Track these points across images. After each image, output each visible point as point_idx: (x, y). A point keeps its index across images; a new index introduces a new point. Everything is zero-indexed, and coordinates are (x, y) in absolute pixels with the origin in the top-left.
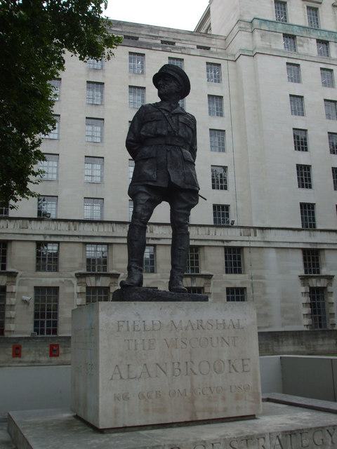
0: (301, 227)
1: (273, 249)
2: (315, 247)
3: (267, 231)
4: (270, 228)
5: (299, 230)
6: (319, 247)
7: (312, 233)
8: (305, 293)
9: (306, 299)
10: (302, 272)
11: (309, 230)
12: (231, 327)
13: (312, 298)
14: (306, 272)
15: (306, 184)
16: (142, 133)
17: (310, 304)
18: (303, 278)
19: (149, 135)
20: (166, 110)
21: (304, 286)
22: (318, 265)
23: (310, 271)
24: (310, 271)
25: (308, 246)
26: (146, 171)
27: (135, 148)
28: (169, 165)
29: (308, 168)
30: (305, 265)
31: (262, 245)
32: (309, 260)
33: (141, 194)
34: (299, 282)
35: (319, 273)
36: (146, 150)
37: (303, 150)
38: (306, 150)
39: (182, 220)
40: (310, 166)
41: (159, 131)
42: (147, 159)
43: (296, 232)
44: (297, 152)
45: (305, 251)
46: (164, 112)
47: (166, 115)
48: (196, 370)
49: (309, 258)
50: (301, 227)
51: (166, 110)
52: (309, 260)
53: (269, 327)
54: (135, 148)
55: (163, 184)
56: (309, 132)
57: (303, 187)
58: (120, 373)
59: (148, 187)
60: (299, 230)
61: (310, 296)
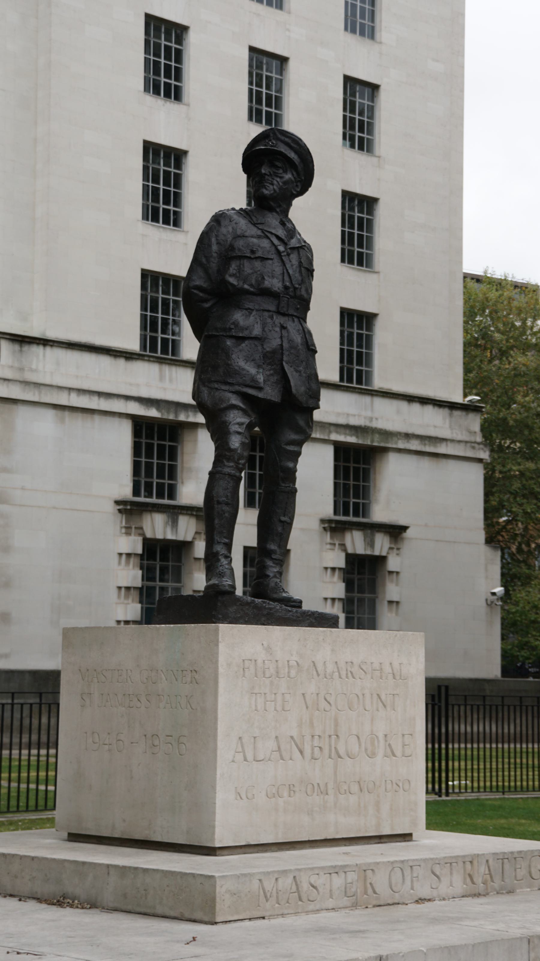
0: (134, 346)
1: (50, 413)
2: (171, 417)
3: (38, 350)
4: (45, 342)
5: (129, 356)
6: (182, 417)
7: (167, 369)
8: (129, 555)
9: (133, 576)
10: (125, 489)
11: (161, 361)
12: (390, 676)
13: (148, 574)
14: (136, 492)
15: (166, 212)
16: (232, 280)
17: (141, 589)
18: (130, 511)
19: (246, 286)
20: (278, 237)
21: (128, 534)
22: (173, 473)
23: (149, 487)
24: (149, 487)
25: (153, 413)
26: (242, 363)
27: (207, 305)
28: (285, 358)
29: (177, 156)
30: (136, 466)
31: (15, 392)
32: (149, 455)
33: (236, 412)
34: (110, 521)
35: (172, 495)
36: (238, 316)
37: (167, 95)
38: (178, 97)
39: (291, 465)
40: (185, 153)
41: (268, 283)
42: (243, 339)
43: (121, 362)
44: (150, 100)
45: (141, 427)
46: (276, 242)
47: (281, 248)
48: (342, 752)
49: (150, 447)
50: (134, 346)
51: (278, 237)
52: (149, 455)
53: (6, 656)
54: (207, 305)
55: (271, 393)
56: (193, 39)
57: (155, 219)
58: (244, 752)
59: (245, 397)
60: (129, 356)
61: (141, 568)
